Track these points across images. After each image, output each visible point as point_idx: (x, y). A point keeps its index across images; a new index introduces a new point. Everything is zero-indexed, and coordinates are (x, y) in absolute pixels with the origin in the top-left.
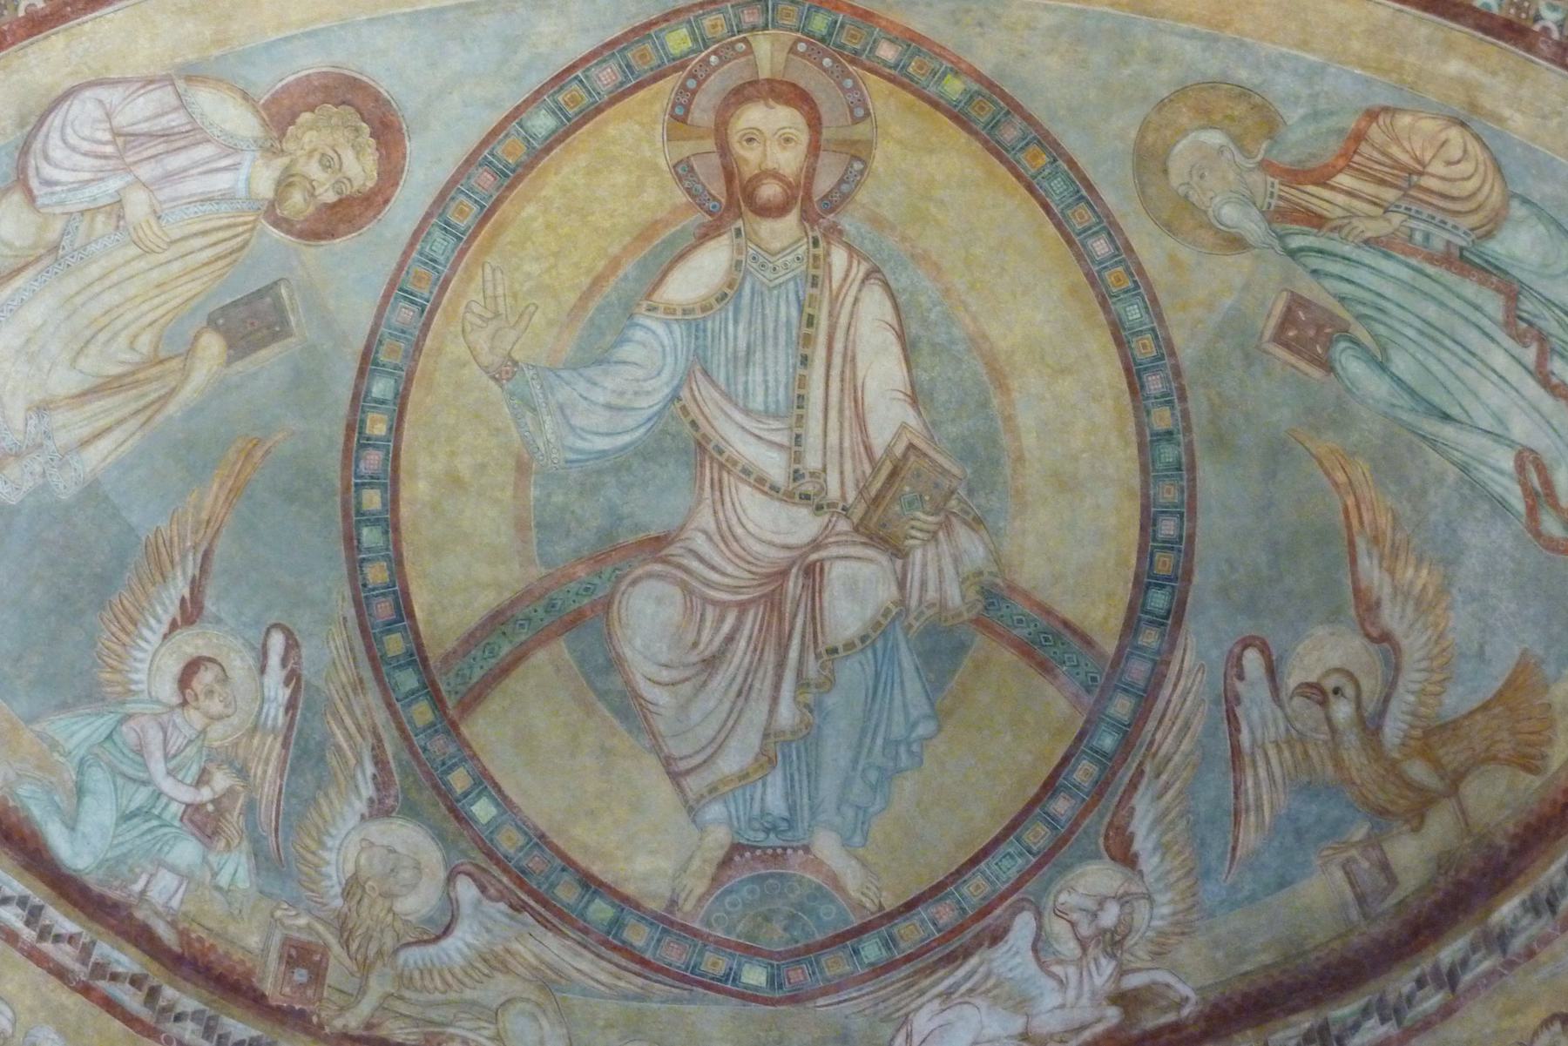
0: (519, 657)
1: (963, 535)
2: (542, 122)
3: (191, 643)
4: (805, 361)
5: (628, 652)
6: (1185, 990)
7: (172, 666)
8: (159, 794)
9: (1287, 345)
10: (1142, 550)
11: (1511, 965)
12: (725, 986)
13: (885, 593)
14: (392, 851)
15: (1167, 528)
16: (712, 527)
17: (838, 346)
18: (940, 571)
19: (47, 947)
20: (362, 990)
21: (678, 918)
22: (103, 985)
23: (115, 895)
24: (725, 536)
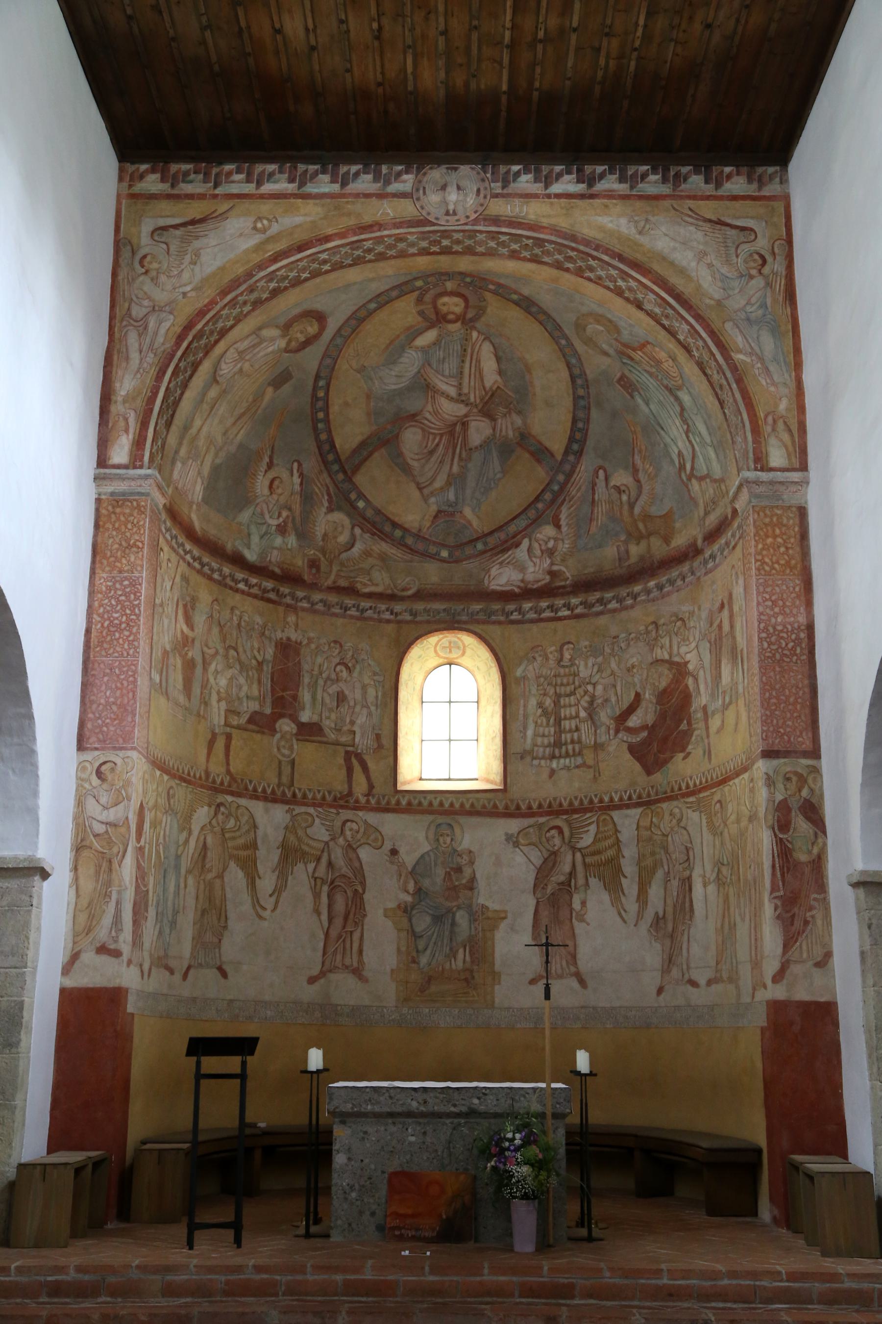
0: (370, 454)
1: (514, 416)
2: (373, 306)
3: (271, 475)
4: (463, 361)
5: (404, 450)
6: (568, 575)
7: (267, 483)
8: (269, 525)
9: (621, 386)
10: (572, 430)
11: (649, 601)
12: (435, 557)
13: (488, 432)
14: (335, 522)
15: (580, 425)
16: (431, 410)
17: (475, 357)
18: (507, 427)
19: (252, 591)
20: (331, 571)
21: (421, 534)
22: (266, 595)
23: (263, 565)
24: (436, 413)
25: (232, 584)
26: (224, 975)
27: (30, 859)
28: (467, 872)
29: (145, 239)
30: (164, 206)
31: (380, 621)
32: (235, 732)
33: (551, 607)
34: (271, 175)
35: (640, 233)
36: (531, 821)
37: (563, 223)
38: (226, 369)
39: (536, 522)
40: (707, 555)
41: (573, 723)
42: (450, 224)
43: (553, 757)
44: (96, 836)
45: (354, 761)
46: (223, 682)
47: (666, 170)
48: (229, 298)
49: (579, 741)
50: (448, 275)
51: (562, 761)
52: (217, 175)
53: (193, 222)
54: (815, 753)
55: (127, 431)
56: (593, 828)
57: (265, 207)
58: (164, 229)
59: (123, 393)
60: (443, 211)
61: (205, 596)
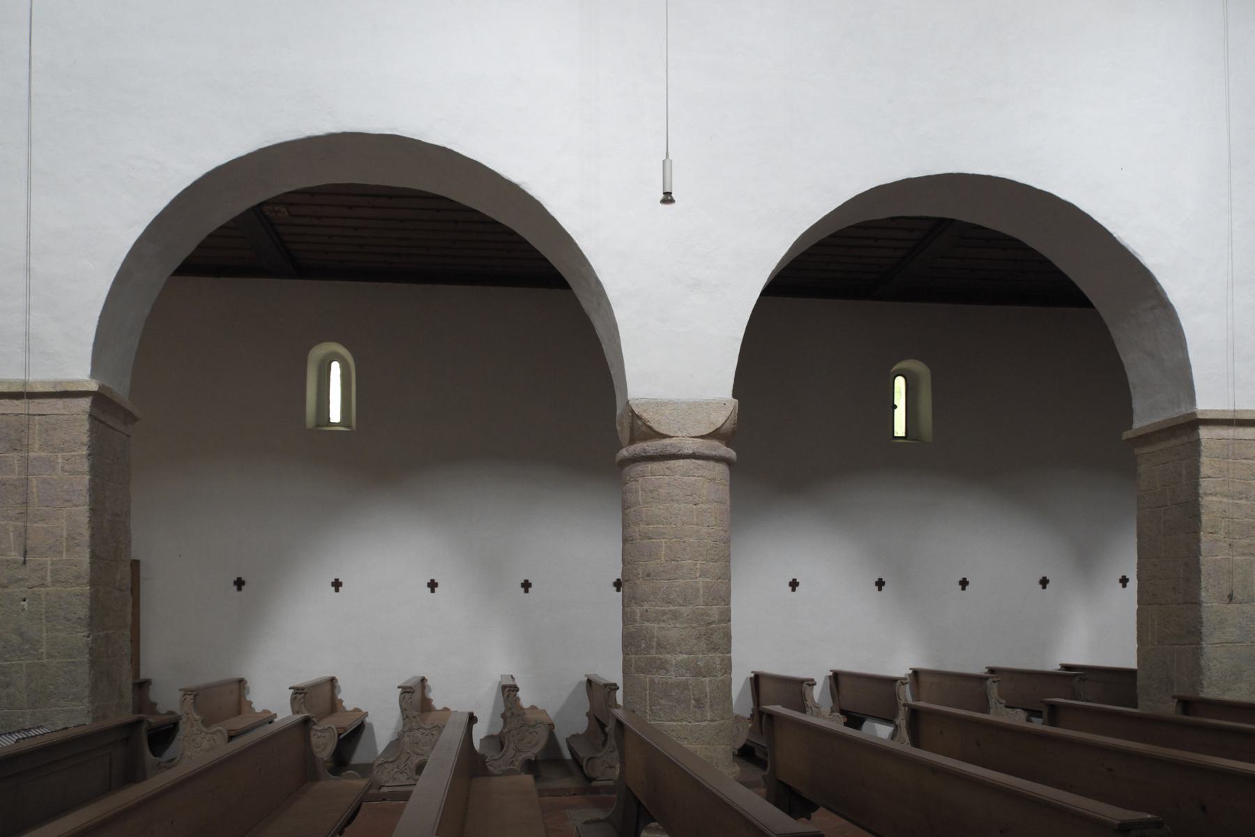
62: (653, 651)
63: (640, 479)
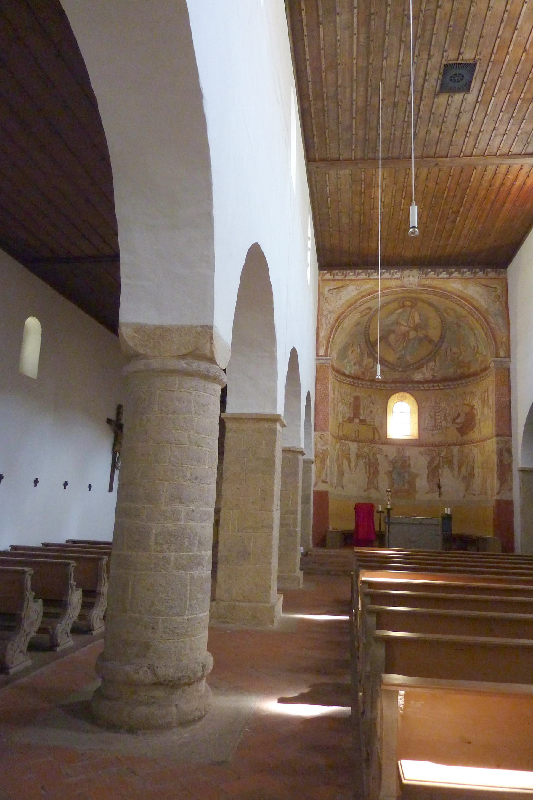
3: (353, 349)
7: (351, 351)
13: (415, 335)
25: (343, 381)
26: (343, 489)
27: (310, 459)
28: (408, 462)
29: (326, 293)
30: (331, 283)
31: (382, 389)
32: (344, 422)
33: (433, 386)
34: (361, 273)
35: (464, 289)
36: (428, 448)
37: (443, 287)
38: (345, 325)
39: (429, 361)
40: (481, 376)
41: (440, 421)
42: (411, 287)
43: (433, 430)
44: (320, 453)
45: (375, 431)
46: (341, 409)
47: (472, 270)
48: (349, 309)
49: (441, 426)
50: (408, 297)
51: (436, 431)
52: (345, 273)
53: (339, 288)
54: (510, 435)
55: (323, 346)
56: (445, 451)
57: (359, 283)
58: (331, 289)
59: (322, 336)
60: (409, 283)
61: (337, 384)
62: (195, 549)
63: (194, 393)
